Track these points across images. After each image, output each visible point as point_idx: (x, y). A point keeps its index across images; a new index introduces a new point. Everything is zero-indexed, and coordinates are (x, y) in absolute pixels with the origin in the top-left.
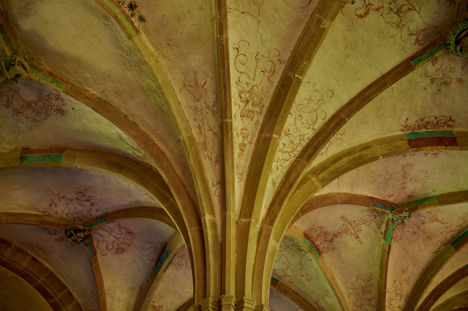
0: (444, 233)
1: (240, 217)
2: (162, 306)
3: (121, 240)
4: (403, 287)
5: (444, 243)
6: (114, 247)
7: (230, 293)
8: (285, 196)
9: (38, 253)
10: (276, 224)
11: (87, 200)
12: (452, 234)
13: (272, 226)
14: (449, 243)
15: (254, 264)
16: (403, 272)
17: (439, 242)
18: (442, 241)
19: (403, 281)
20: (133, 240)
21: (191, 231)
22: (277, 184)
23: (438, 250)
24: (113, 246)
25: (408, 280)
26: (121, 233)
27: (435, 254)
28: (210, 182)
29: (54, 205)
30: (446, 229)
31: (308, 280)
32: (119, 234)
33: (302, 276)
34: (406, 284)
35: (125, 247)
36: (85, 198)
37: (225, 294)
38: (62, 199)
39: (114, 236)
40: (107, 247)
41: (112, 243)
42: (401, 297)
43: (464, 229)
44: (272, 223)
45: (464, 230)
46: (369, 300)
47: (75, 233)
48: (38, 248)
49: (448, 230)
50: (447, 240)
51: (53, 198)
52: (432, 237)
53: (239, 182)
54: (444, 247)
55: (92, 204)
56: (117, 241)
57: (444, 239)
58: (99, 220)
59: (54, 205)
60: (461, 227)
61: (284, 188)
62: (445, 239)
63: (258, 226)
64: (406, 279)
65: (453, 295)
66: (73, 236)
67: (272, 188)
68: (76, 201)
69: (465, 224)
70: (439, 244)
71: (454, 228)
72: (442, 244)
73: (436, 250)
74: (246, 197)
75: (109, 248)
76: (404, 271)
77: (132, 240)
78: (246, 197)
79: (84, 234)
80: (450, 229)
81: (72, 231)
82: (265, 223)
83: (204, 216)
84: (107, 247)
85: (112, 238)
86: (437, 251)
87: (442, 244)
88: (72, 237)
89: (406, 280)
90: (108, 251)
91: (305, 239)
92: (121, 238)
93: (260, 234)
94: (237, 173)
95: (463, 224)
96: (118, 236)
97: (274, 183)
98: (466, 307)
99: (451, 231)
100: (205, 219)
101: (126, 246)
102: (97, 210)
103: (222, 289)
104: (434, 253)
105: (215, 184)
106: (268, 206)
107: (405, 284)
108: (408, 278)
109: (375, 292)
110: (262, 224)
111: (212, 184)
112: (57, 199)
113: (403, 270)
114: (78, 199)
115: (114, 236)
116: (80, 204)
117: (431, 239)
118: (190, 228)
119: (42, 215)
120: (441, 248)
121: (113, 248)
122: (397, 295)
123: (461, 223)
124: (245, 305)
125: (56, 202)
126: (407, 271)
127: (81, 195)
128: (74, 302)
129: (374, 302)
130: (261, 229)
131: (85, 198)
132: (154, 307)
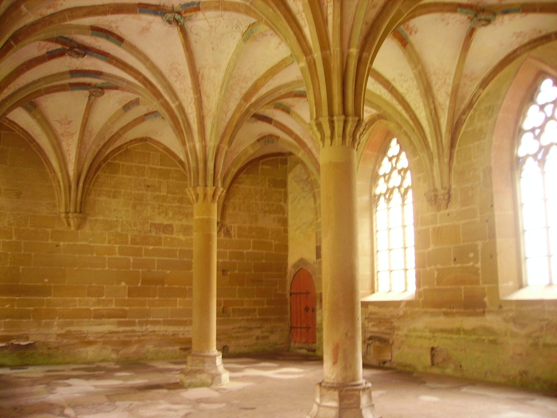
31: (213, 49)
33: (212, 43)
46: (242, 88)
129: (244, 91)
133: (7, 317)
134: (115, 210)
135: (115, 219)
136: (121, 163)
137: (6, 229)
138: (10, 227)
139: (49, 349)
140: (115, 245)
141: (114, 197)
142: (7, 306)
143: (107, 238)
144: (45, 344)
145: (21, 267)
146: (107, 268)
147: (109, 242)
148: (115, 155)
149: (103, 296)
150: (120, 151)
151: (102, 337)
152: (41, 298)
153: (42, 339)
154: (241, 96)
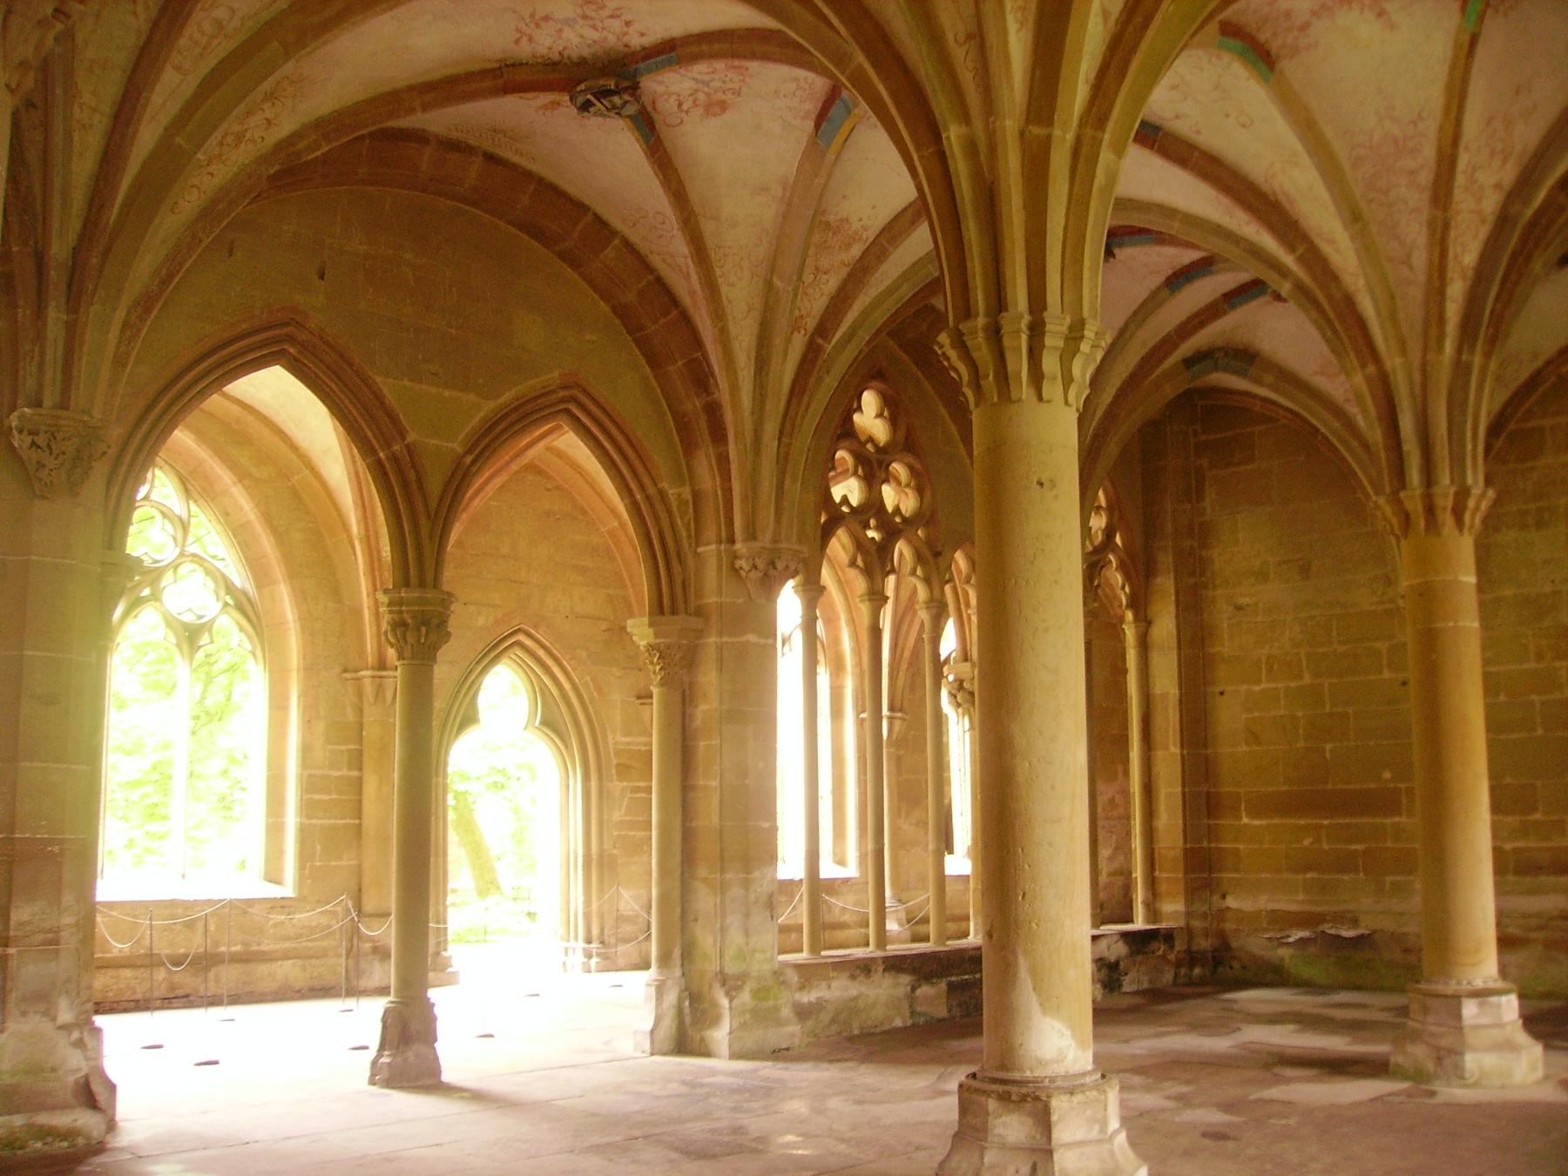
1: (1028, 121)
2: (847, 220)
3: (717, 84)
6: (698, 102)
7: (1016, 305)
8: (1133, 50)
9: (496, 142)
10: (1110, 126)
11: (612, 17)
13: (1104, 131)
15: (1066, 227)
20: (747, 80)
21: (921, 158)
22: (1113, 18)
24: (694, 101)
26: (711, 70)
28: (950, 36)
29: (525, 39)
31: (1243, 126)
32: (707, 73)
35: (728, 97)
36: (605, 13)
37: (1007, 310)
38: (542, 24)
39: (694, 79)
40: (680, 105)
41: (691, 95)
42: (1505, 160)
44: (1101, 122)
46: (1412, 173)
47: (599, 101)
48: (495, 131)
51: (522, 25)
53: (1018, 31)
55: (628, 24)
56: (706, 90)
58: (652, 60)
59: (525, 39)
61: (1131, 29)
63: (1070, 137)
66: (594, 105)
67: (1100, 28)
68: (581, 22)
74: (1038, 72)
75: (685, 107)
77: (743, 81)
78: (1038, 72)
79: (621, 98)
81: (589, 97)
82: (1087, 122)
83: (947, 129)
84: (680, 105)
85: (691, 84)
88: (592, 109)
90: (684, 114)
91: (1225, 39)
92: (713, 80)
93: (1076, 152)
94: (1012, 8)
96: (707, 78)
97: (1105, 14)
100: (948, 138)
101: (729, 94)
102: (642, 35)
103: (999, 302)
105: (961, 38)
106: (1092, 76)
109: (1429, 152)
110: (1081, 126)
111: (956, 40)
112: (532, 25)
114: (585, 17)
115: (694, 79)
116: (594, 28)
118: (918, 150)
119: (500, 68)
121: (697, 106)
122: (1492, 154)
124: (1048, 327)
125: (529, 31)
127: (594, 7)
128: (617, 242)
129: (1426, 177)
130: (1078, 140)
131: (605, 13)
132: (828, 224)
133: (1308, 868)
134: (1546, 562)
135: (1548, 589)
136: (1548, 422)
137: (1288, 659)
138: (1296, 651)
139: (1406, 951)
140: (1557, 664)
141: (1539, 525)
142: (1306, 842)
143: (1531, 646)
144: (1398, 938)
145: (1328, 747)
146: (1540, 732)
147: (1540, 656)
148: (1527, 405)
149: (1534, 809)
150: (1541, 390)
151: (1541, 928)
152: (1378, 820)
153: (1387, 924)
154: (1426, 196)
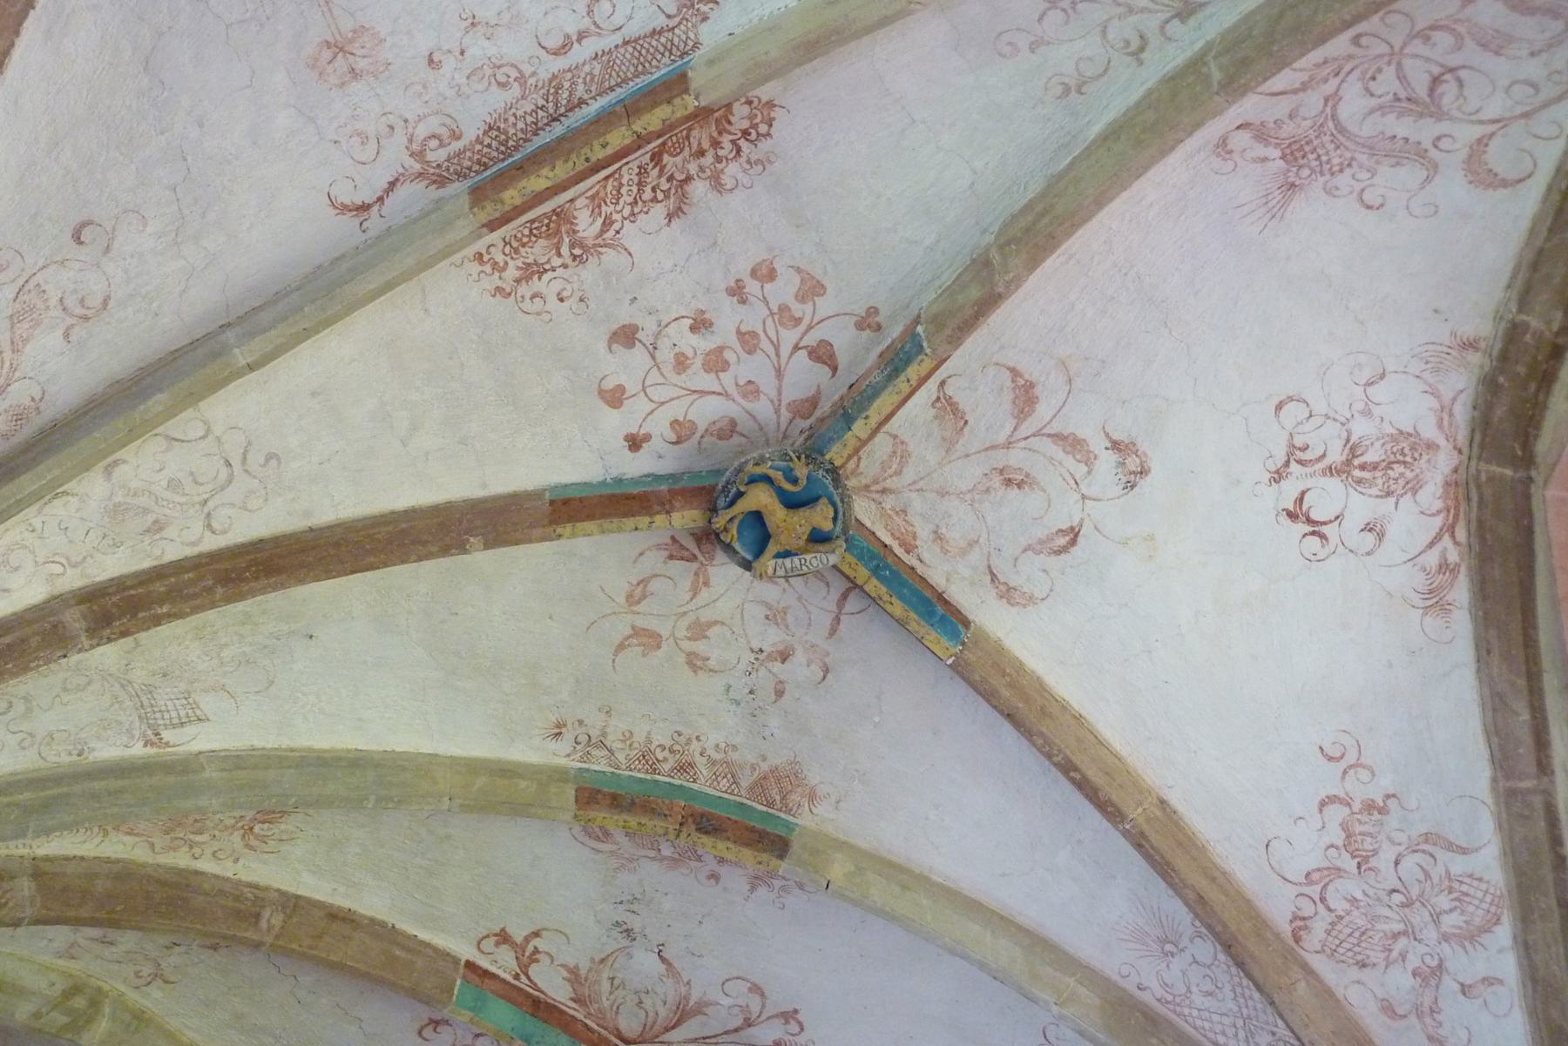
0: (449, 64)
4: (25, 341)
5: (430, 156)
12: (498, 99)
14: (462, 175)
16: (77, 238)
17: (400, 138)
18: (422, 131)
19: (53, 302)
23: (380, 199)
25: (86, 318)
27: (349, 222)
30: (467, 40)
34: (66, 335)
43: (580, 91)
45: (582, 102)
49: (479, 49)
50: (457, 146)
52: (361, 64)
54: (419, 186)
57: (433, 125)
60: (560, 63)
62: (444, 132)
64: (82, 301)
65: (427, 747)
69: (591, 46)
70: (396, 157)
71: (514, 48)
72: (417, 167)
73: (366, 196)
76: (86, 235)
80: (492, 51)
86: (365, 207)
87: (417, 167)
89: (79, 311)
95: (581, 36)
98: (523, 983)
99: (497, 74)
104: (345, 208)
107: (59, 333)
108: (95, 302)
113: (84, 225)
117: (354, 74)
120: (402, 192)
123: (572, 30)
126: (108, 249)
